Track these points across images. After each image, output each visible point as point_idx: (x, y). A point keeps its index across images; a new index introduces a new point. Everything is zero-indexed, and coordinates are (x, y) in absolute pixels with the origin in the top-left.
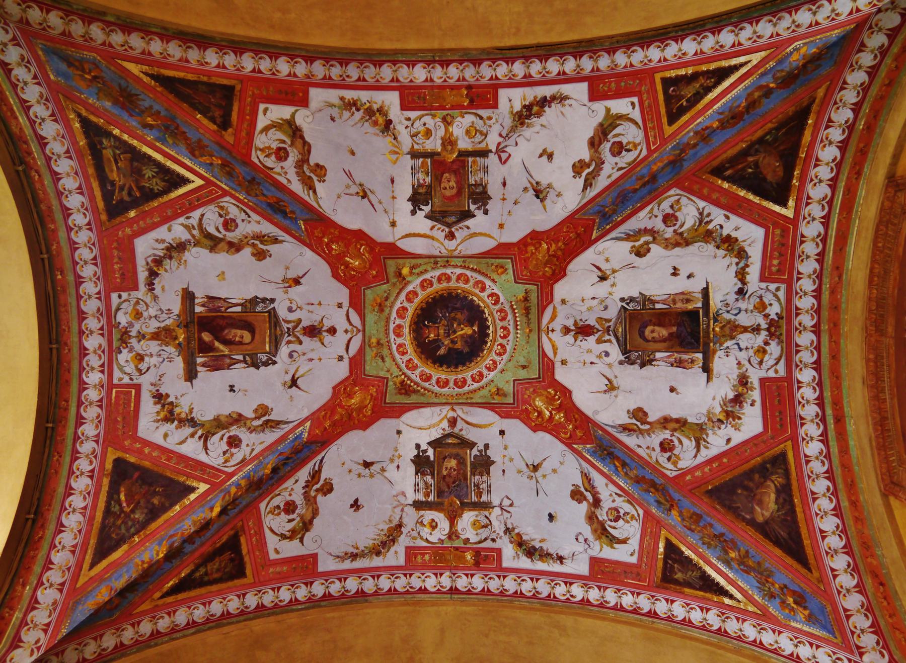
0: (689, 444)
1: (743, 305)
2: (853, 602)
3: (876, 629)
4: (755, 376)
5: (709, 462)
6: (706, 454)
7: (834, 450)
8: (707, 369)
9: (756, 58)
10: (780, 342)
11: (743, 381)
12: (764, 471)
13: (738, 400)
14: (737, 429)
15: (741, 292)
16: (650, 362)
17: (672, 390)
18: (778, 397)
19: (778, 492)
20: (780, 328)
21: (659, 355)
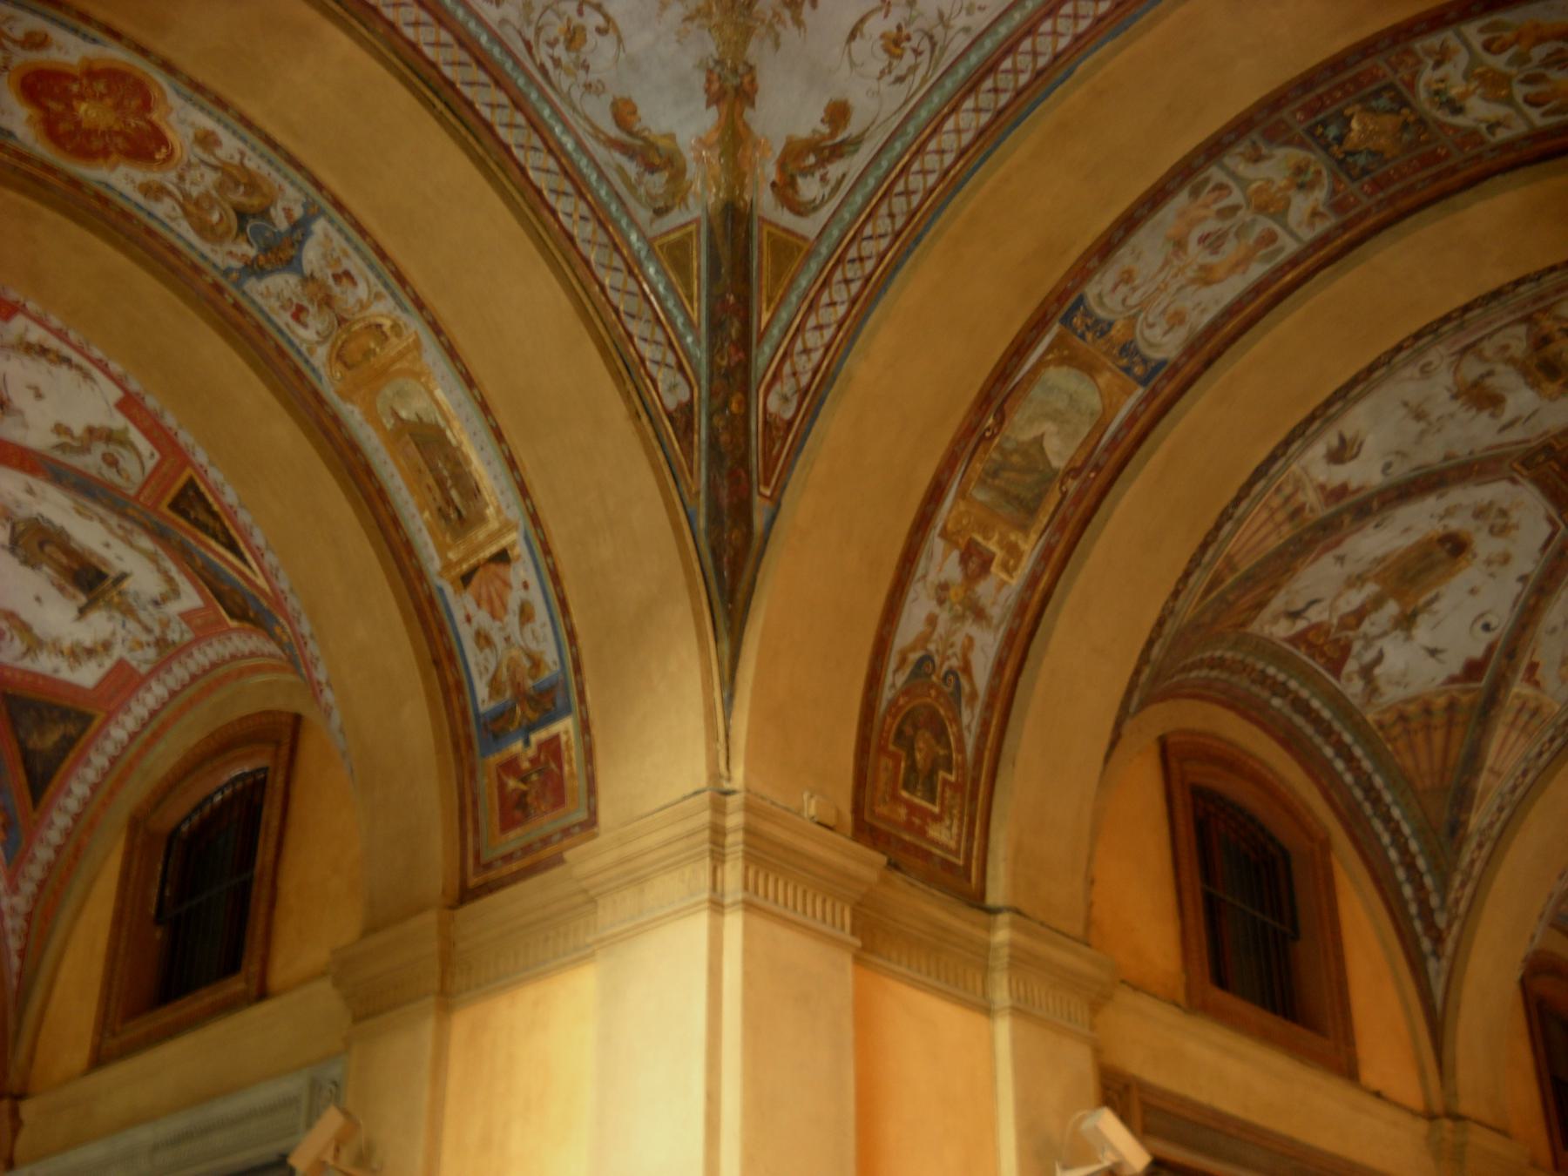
0: (18, 646)
1: (150, 608)
2: (43, 854)
3: (41, 885)
4: (118, 651)
5: (26, 672)
6: (27, 664)
7: (133, 749)
8: (82, 612)
9: (261, 581)
10: (159, 654)
11: (107, 646)
12: (65, 714)
13: (90, 652)
14: (72, 669)
15: (156, 603)
16: (33, 567)
17: (38, 599)
18: (123, 682)
19: (64, 737)
20: (168, 652)
21: (45, 569)
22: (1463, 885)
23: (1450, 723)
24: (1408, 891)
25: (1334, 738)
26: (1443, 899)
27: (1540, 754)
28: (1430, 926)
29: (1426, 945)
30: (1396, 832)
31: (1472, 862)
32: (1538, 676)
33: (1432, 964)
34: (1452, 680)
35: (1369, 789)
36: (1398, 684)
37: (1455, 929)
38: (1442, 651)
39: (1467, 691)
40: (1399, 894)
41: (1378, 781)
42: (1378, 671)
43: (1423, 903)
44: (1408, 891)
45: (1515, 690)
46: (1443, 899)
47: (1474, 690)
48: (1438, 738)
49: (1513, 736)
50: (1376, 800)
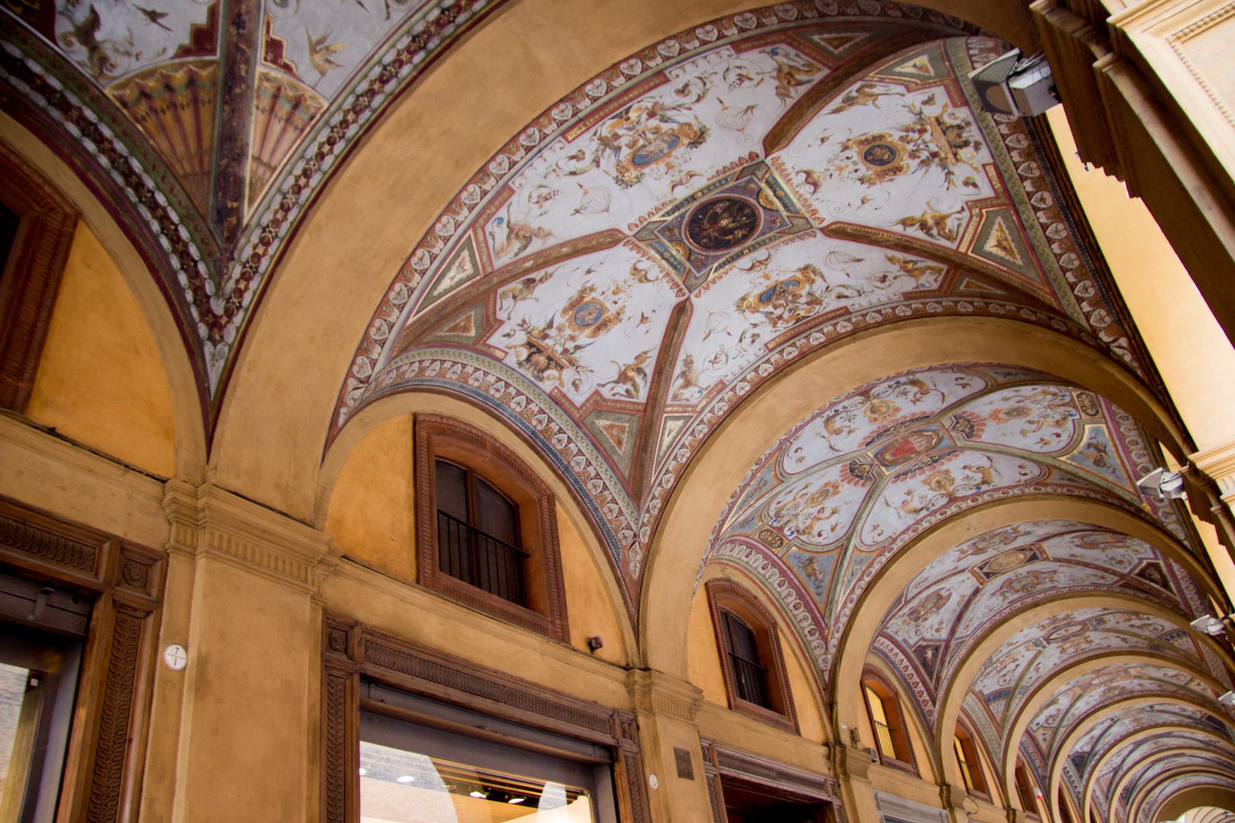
22: (245, 277)
23: (195, 101)
24: (183, 279)
25: (75, 114)
26: (219, 287)
27: (321, 156)
28: (206, 312)
29: (203, 330)
30: (164, 219)
31: (257, 257)
32: (286, 59)
33: (208, 348)
34: (184, 51)
35: (128, 173)
36: (128, 54)
37: (239, 318)
38: (162, 15)
39: (205, 65)
40: (176, 282)
41: (136, 165)
42: (99, 36)
43: (198, 290)
44: (183, 279)
45: (260, 69)
46: (219, 287)
47: (212, 63)
48: (187, 116)
49: (277, 127)
50: (139, 186)
